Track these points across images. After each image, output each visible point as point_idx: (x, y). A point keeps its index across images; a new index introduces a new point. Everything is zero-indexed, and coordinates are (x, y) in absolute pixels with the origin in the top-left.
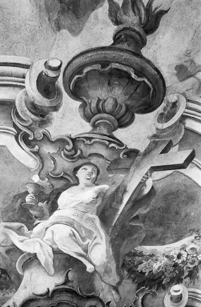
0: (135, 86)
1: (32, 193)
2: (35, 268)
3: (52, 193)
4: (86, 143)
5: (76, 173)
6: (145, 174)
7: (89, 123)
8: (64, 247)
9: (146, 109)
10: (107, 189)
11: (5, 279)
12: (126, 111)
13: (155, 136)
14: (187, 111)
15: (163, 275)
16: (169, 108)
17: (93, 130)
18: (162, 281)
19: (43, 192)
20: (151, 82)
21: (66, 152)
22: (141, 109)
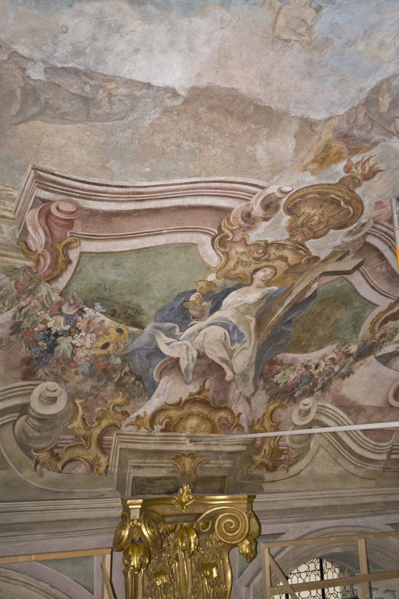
5: (254, 274)
9: (341, 226)
11: (139, 386)
12: (324, 227)
14: (371, 229)
15: (297, 387)
18: (295, 393)
19: (212, 291)
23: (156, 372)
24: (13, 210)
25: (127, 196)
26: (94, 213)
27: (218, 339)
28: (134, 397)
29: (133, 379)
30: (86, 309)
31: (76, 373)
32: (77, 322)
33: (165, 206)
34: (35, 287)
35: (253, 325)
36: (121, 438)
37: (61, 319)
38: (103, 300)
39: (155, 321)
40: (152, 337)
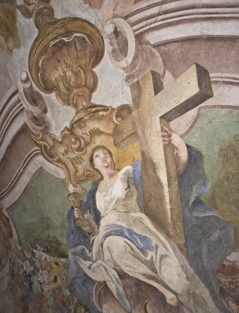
0: (73, 46)
3: (88, 198)
6: (162, 132)
7: (70, 105)
8: (127, 268)
9: (96, 58)
10: (131, 170)
12: (85, 73)
13: (128, 79)
14: (135, 28)
16: (114, 41)
17: (76, 110)
19: (81, 200)
20: (80, 32)
22: (93, 62)
23: (96, 301)
27: (124, 250)
35: (147, 222)
40: (76, 262)
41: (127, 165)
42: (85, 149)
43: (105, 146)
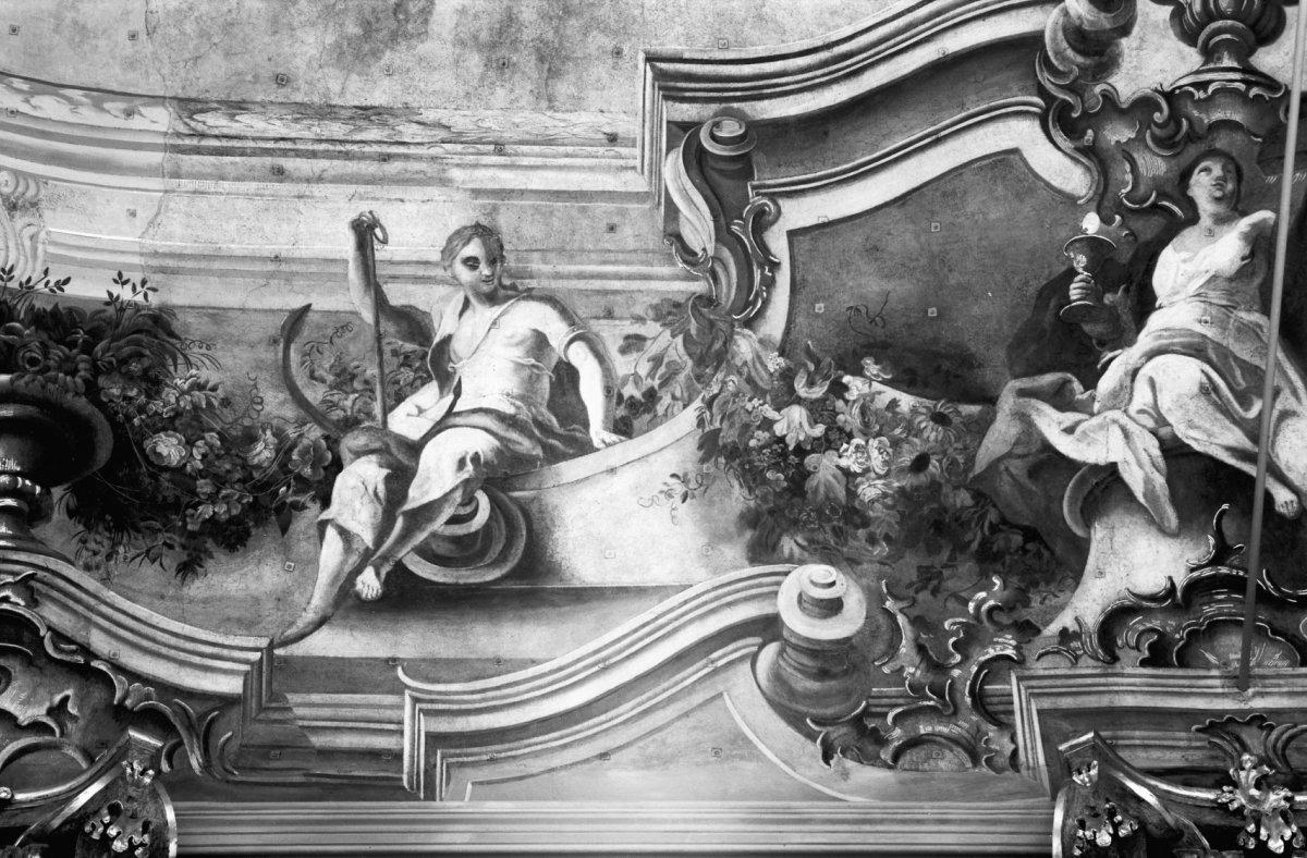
1: (1085, 269)
2: (1120, 511)
3: (1135, 257)
4: (1197, 97)
8: (1193, 433)
10: (1272, 222)
11: (1039, 555)
21: (1157, 131)
23: (1070, 512)
24: (638, 163)
25: (826, 70)
26: (781, 126)
28: (1035, 584)
29: (1017, 539)
30: (847, 379)
31: (872, 540)
32: (838, 414)
33: (906, 71)
34: (725, 343)
36: (1033, 687)
37: (797, 414)
38: (880, 349)
39: (1016, 377)
40: (1024, 418)
41: (1266, 209)
42: (1180, 147)
43: (1234, 154)
